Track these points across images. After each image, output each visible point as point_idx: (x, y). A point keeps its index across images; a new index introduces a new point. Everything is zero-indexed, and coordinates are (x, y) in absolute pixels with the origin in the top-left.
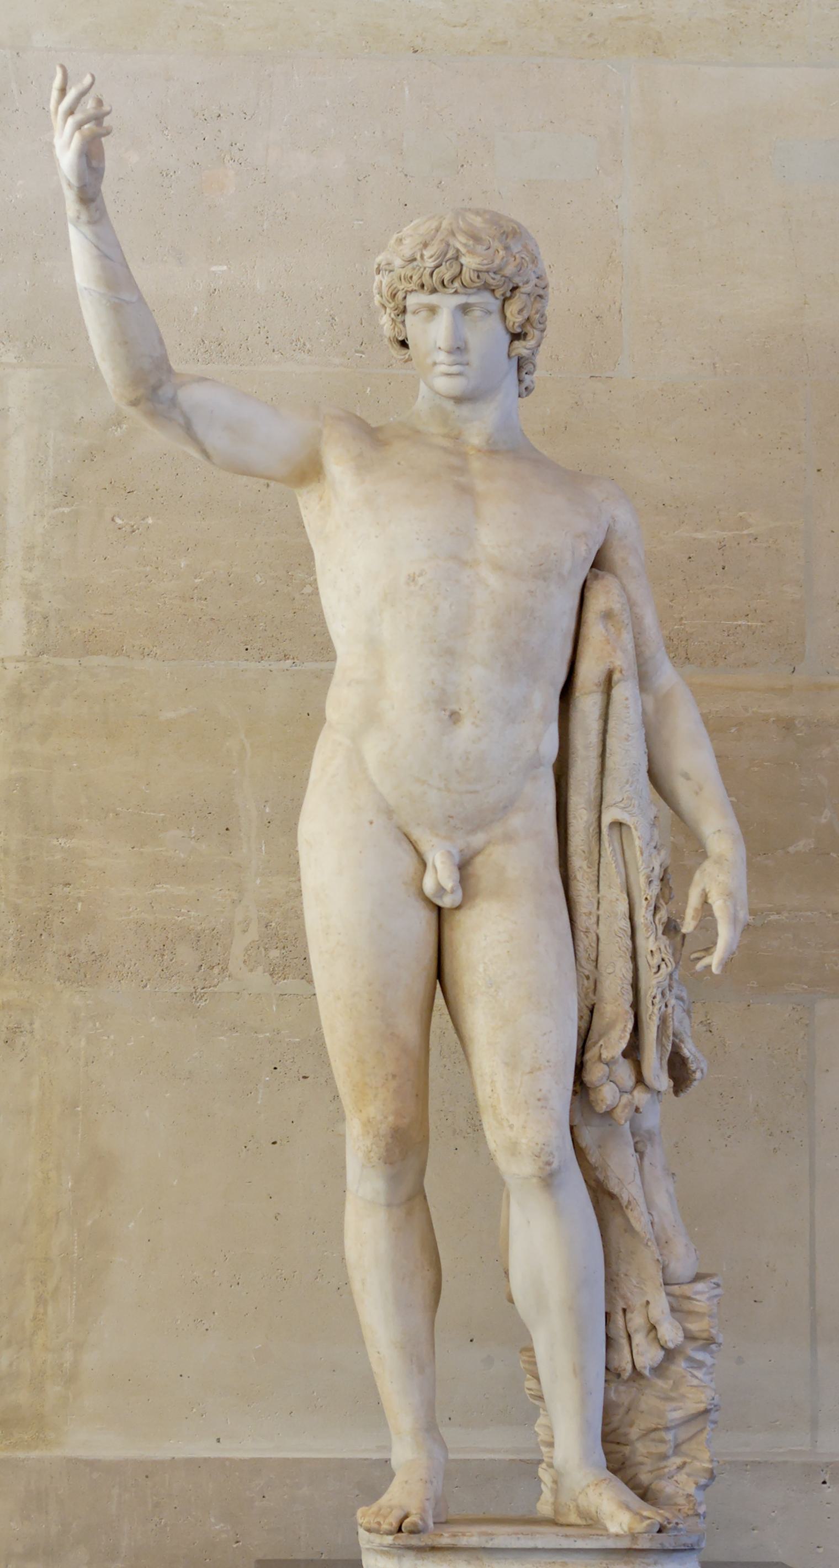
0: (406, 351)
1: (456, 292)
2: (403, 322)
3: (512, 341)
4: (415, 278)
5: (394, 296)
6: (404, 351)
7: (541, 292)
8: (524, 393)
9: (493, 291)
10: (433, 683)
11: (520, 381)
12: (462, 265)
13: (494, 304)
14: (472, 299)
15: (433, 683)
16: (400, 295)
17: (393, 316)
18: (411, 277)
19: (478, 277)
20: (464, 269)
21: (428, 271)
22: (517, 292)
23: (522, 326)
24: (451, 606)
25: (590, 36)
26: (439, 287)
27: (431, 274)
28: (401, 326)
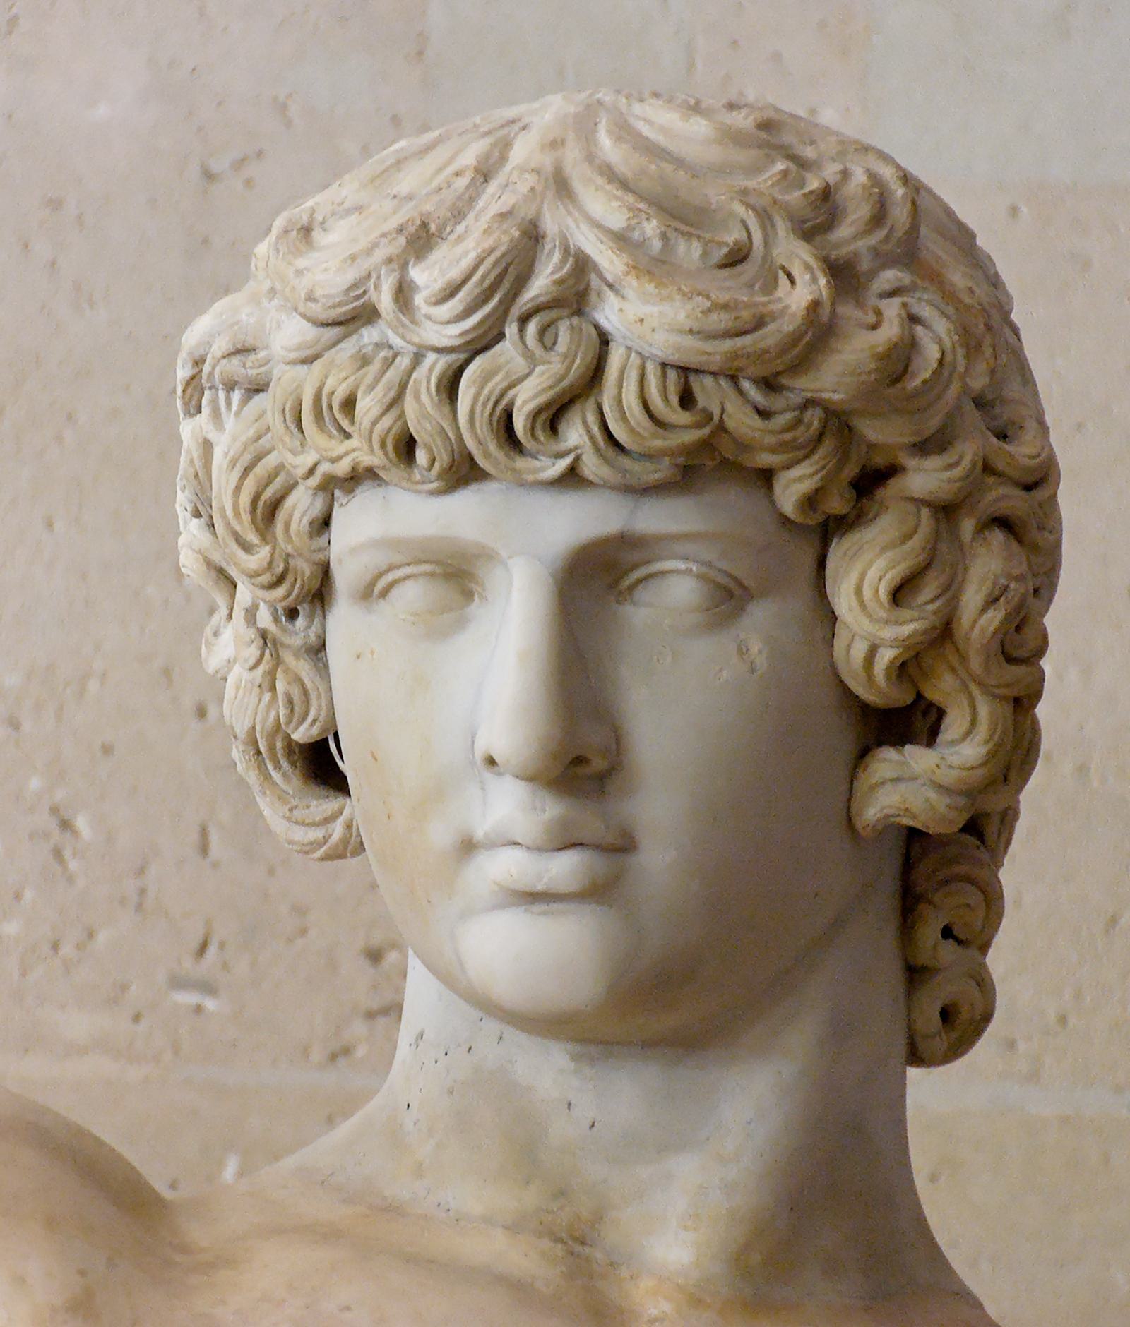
1: (572, 478)
2: (318, 650)
4: (367, 405)
5: (267, 513)
6: (323, 804)
11: (915, 974)
16: (301, 505)
17: (264, 618)
18: (349, 404)
19: (687, 400)
20: (616, 358)
21: (435, 366)
27: (450, 386)
28: (303, 668)
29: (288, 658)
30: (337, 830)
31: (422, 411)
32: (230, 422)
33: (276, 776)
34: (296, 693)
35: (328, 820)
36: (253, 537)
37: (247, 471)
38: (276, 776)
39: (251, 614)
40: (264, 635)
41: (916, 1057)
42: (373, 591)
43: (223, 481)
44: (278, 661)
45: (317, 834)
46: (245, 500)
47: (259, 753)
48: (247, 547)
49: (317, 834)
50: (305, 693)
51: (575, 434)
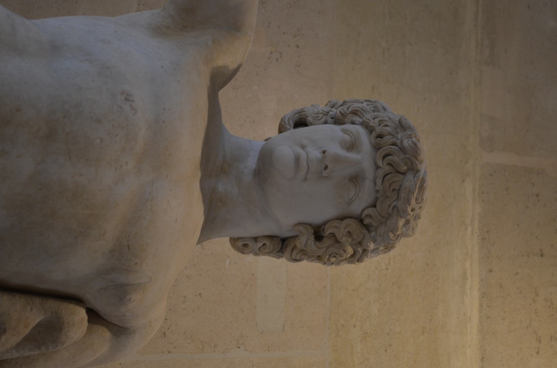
0: (292, 126)
1: (378, 167)
2: (326, 123)
3: (310, 225)
7: (358, 256)
8: (240, 244)
9: (374, 206)
10: (18, 110)
11: (256, 239)
12: (404, 174)
13: (357, 208)
14: (368, 185)
15: (18, 110)
16: (357, 119)
17: (331, 113)
18: (386, 126)
19: (394, 190)
22: (365, 231)
23: (333, 235)
24: (102, 140)
25: (343, 326)
26: (382, 152)
27: (394, 144)
28: (324, 119)
29: (325, 117)
30: (288, 127)
31: (387, 138)
32: (368, 107)
33: (297, 116)
34: (319, 118)
35: (290, 125)
36: (350, 110)
37: (362, 109)
38: (297, 116)
39: (331, 111)
40: (328, 113)
41: (234, 241)
42: (345, 131)
43: (359, 105)
44: (324, 115)
45: (287, 123)
46: (358, 109)
47: (300, 113)
48: (348, 108)
49: (287, 123)
50: (319, 120)
51: (387, 169)
